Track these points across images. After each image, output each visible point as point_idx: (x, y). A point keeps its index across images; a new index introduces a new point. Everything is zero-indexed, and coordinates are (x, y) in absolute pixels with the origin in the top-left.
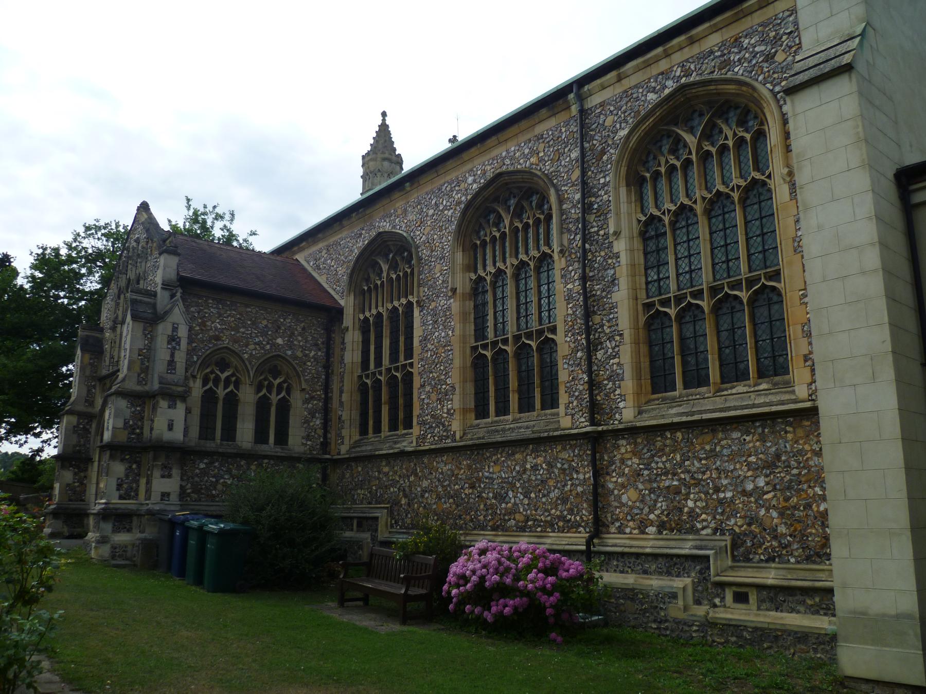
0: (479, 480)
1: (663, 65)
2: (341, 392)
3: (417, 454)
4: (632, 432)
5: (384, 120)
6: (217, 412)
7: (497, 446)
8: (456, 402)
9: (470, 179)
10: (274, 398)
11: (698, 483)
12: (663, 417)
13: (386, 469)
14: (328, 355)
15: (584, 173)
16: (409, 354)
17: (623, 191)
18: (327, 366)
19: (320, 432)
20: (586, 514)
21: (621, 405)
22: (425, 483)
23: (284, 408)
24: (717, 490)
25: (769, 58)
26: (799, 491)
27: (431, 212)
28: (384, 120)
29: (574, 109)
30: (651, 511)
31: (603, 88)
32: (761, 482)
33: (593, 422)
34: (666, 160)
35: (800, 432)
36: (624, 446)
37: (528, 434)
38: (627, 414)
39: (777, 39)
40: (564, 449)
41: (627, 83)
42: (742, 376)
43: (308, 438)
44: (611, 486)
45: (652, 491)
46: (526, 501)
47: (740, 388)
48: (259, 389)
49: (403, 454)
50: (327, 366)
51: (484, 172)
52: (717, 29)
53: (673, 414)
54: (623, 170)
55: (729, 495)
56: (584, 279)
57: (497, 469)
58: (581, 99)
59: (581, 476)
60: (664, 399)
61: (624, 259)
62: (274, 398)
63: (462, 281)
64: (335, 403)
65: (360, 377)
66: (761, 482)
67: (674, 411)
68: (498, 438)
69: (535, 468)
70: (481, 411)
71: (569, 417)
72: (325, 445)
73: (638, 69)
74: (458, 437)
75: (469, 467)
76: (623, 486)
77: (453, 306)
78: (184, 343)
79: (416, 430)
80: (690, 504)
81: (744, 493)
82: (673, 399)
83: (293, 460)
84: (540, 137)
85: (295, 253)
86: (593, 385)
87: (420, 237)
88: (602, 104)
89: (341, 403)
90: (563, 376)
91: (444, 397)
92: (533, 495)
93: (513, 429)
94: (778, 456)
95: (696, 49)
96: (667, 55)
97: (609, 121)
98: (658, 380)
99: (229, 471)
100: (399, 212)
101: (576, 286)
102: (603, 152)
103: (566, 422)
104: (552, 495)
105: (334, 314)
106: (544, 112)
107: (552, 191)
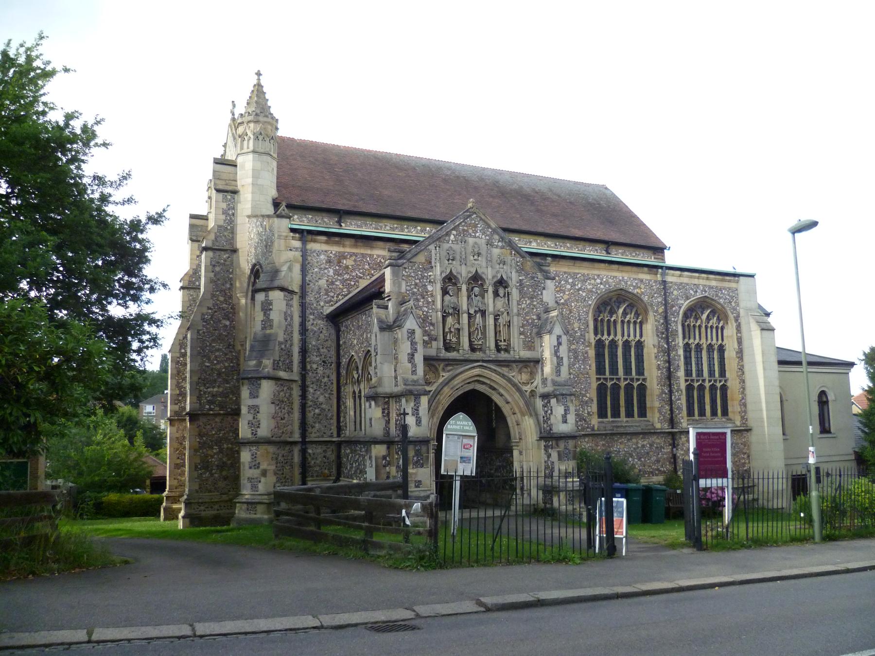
1: (696, 281)
5: (259, 79)
7: (622, 434)
9: (598, 281)
25: (730, 302)
28: (259, 79)
31: (673, 275)
37: (639, 430)
52: (715, 280)
57: (622, 446)
58: (663, 275)
68: (621, 430)
69: (643, 446)
70: (602, 414)
74: (596, 428)
77: (590, 352)
84: (642, 281)
95: (707, 283)
106: (646, 269)
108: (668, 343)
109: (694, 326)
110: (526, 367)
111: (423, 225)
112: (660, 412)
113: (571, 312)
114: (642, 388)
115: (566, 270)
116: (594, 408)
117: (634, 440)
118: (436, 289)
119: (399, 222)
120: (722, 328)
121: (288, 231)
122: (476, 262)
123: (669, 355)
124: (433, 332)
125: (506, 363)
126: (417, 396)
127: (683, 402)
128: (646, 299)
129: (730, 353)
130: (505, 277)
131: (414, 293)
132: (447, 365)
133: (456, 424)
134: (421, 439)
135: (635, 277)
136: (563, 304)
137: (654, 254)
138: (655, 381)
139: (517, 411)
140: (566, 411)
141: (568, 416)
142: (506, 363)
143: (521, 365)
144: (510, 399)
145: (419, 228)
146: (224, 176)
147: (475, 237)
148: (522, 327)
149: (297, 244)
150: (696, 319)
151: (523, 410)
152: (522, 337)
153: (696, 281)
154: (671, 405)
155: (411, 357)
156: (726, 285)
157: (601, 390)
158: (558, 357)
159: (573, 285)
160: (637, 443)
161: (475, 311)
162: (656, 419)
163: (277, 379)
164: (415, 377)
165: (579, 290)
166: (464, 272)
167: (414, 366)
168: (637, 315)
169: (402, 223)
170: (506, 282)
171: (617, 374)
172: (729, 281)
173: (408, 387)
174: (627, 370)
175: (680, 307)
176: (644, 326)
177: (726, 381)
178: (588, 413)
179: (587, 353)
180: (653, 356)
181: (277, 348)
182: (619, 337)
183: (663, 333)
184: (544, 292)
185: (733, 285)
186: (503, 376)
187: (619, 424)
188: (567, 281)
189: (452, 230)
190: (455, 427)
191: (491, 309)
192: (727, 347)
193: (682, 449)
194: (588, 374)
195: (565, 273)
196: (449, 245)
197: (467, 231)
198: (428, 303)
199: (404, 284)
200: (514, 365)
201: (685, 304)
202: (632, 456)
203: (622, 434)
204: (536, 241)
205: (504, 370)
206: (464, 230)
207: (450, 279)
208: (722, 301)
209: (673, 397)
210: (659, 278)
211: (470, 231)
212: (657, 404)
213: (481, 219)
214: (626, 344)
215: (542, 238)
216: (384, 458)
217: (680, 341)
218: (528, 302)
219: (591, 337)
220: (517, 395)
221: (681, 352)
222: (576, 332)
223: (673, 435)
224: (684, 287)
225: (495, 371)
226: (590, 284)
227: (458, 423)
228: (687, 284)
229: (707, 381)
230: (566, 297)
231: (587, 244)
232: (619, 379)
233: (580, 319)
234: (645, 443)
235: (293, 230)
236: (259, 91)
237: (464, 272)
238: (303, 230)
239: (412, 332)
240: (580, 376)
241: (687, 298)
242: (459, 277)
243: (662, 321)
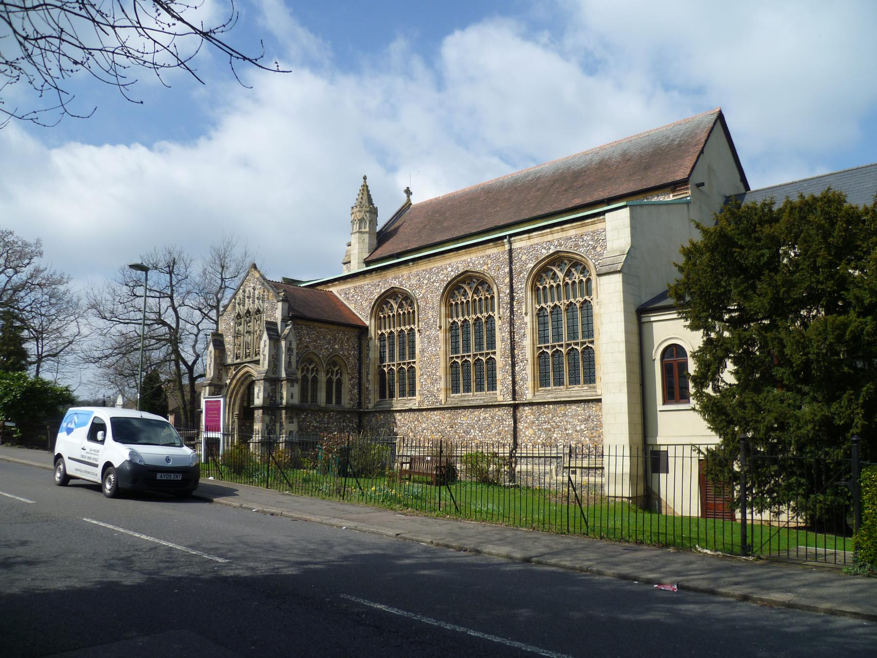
0: (455, 424)
2: (368, 374)
3: (420, 410)
4: (531, 404)
6: (307, 386)
8: (442, 384)
9: (450, 269)
10: (335, 378)
11: (558, 427)
14: (360, 353)
16: (412, 355)
17: (529, 293)
18: (360, 360)
19: (357, 396)
20: (510, 440)
22: (424, 425)
23: (339, 383)
24: (566, 430)
25: (594, 248)
27: (426, 282)
29: (507, 247)
31: (521, 240)
32: (583, 427)
33: (514, 399)
34: (549, 282)
37: (481, 403)
38: (529, 396)
39: (597, 241)
43: (351, 400)
45: (539, 430)
47: (576, 388)
48: (327, 374)
49: (411, 410)
50: (360, 360)
51: (457, 268)
53: (549, 398)
54: (530, 283)
57: (465, 419)
61: (529, 326)
62: (335, 378)
63: (445, 322)
64: (364, 380)
65: (380, 366)
66: (583, 427)
68: (465, 404)
69: (485, 419)
71: (502, 394)
72: (360, 404)
73: (538, 236)
75: (450, 418)
78: (295, 351)
79: (418, 398)
82: (549, 391)
83: (344, 412)
85: (329, 287)
86: (514, 383)
87: (418, 294)
88: (520, 248)
89: (368, 381)
90: (499, 376)
91: (434, 382)
94: (589, 417)
97: (524, 258)
98: (542, 380)
99: (315, 419)
100: (405, 277)
101: (507, 335)
102: (521, 272)
103: (500, 398)
105: (364, 330)
107: (495, 287)
112: (502, 384)
114: (491, 362)
115: (424, 268)
135: (482, 254)
156: (590, 228)
157: (453, 367)
159: (429, 279)
172: (593, 223)
179: (438, 336)
185: (600, 226)
202: (473, 427)
230: (424, 291)
236: (365, 189)
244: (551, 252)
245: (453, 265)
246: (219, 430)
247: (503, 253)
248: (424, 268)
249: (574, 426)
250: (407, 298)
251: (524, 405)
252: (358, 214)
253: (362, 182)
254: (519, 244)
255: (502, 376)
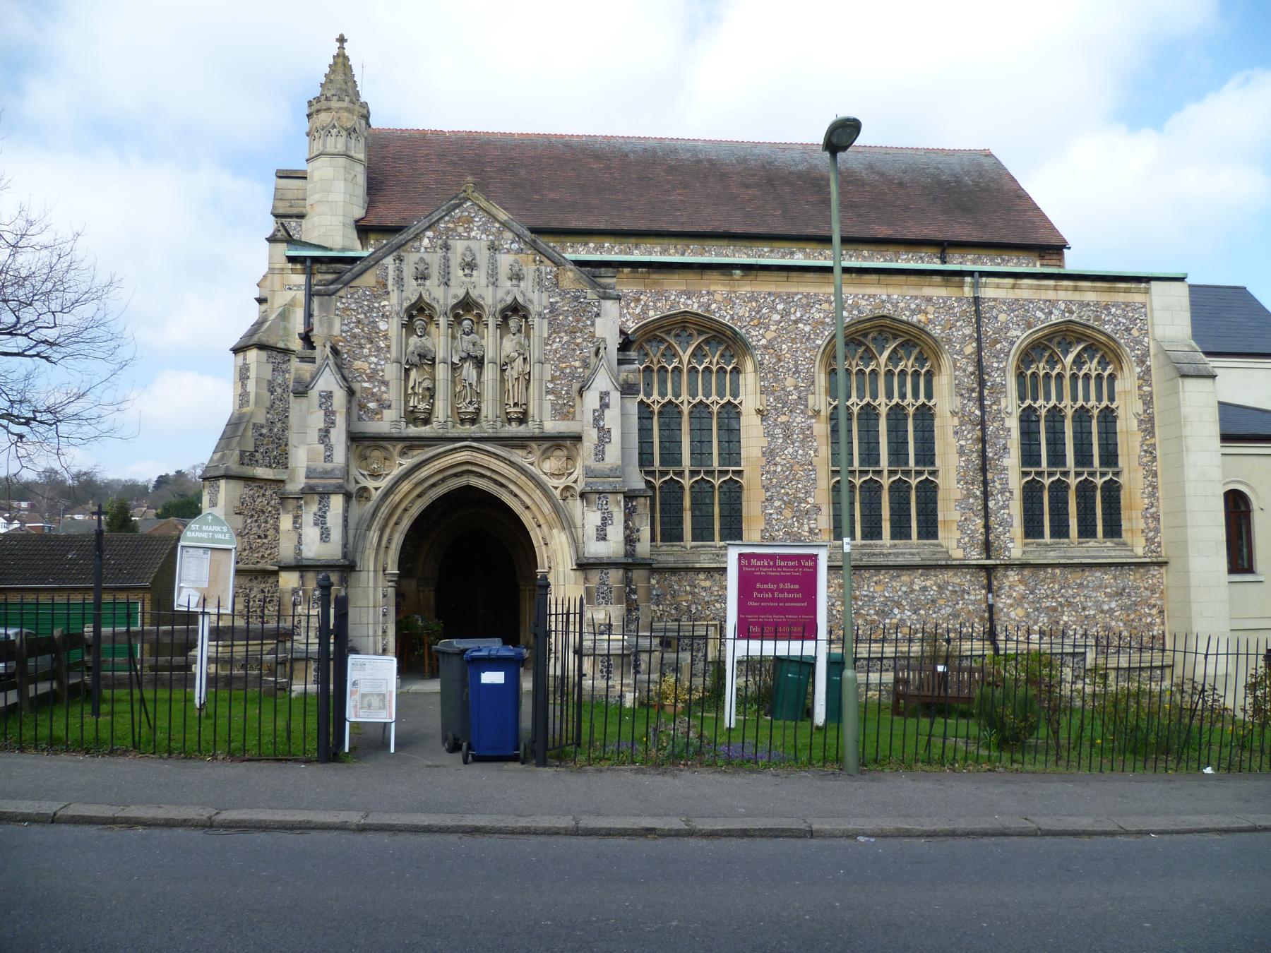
1: (1051, 295)
7: (878, 568)
11: (1070, 604)
12: (1046, 558)
13: (708, 584)
15: (979, 350)
21: (1011, 545)
24: (1084, 609)
25: (1128, 330)
26: (1136, 611)
27: (776, 317)
30: (1036, 623)
31: (998, 286)
35: (1138, 576)
36: (1013, 576)
37: (916, 560)
40: (955, 575)
41: (1018, 294)
42: (1093, 534)
44: (1001, 605)
45: (1037, 609)
46: (914, 617)
47: (1092, 543)
52: (1094, 290)
53: (1052, 557)
55: (1092, 612)
56: (983, 441)
57: (878, 588)
59: (972, 598)
60: (1039, 545)
66: (1113, 605)
67: (1051, 554)
68: (880, 561)
69: (924, 589)
73: (1031, 287)
76: (1011, 605)
80: (1065, 618)
81: (1102, 611)
84: (929, 300)
87: (757, 337)
88: (995, 300)
92: (922, 612)
93: (896, 555)
94: (1124, 589)
95: (1077, 296)
96: (1055, 288)
97: (1002, 317)
98: (1032, 529)
100: (718, 297)
102: (996, 341)
103: (957, 554)
104: (943, 612)
106: (937, 279)
108: (982, 407)
109: (1047, 376)
110: (559, 447)
111: (597, 239)
112: (961, 528)
113: (780, 360)
114: (929, 492)
115: (772, 289)
116: (824, 521)
117: (905, 578)
118: (391, 327)
119: (557, 239)
120: (1112, 377)
121: (284, 259)
122: (468, 279)
123: (983, 430)
124: (385, 396)
125: (519, 442)
126: (324, 495)
127: (1016, 509)
128: (936, 331)
129: (1127, 425)
130: (520, 300)
131: (354, 336)
132: (411, 448)
133: (201, 530)
134: (324, 563)
135: (915, 293)
136: (765, 347)
137: (1042, 257)
138: (953, 476)
139: (542, 521)
140: (605, 521)
141: (609, 529)
142: (519, 442)
143: (546, 445)
144: (529, 502)
145: (592, 245)
146: (289, 195)
147: (469, 238)
148: (552, 381)
149: (300, 279)
150: (1052, 362)
151: (550, 518)
152: (551, 397)
153: (1051, 295)
154: (986, 517)
155: (325, 435)
156: (1121, 298)
158: (600, 429)
160: (912, 583)
161: (461, 359)
162: (954, 540)
163: (249, 480)
164: (329, 466)
165: (796, 322)
166: (442, 296)
167: (329, 448)
168: (921, 360)
169: (563, 239)
170: (524, 308)
171: (877, 463)
172: (1127, 291)
173: (313, 482)
174: (898, 454)
175: (1012, 343)
176: (935, 380)
177: (1117, 474)
178: (811, 531)
179: (810, 428)
180: (950, 431)
181: (250, 433)
182: (882, 399)
183: (973, 390)
184: (598, 320)
185: (1137, 298)
186: (512, 464)
187: (877, 551)
188: (773, 309)
189: (426, 229)
190: (199, 535)
191: (489, 355)
192: (1120, 413)
193: (1009, 597)
194: (811, 463)
195: (770, 294)
196: (419, 255)
197: (454, 230)
198: (379, 349)
199: (337, 321)
200: (534, 445)
201: (1021, 337)
202: (898, 605)
203: (878, 568)
204: (802, 250)
205: (518, 456)
206: (448, 229)
207: (418, 313)
208: (1108, 328)
209: (991, 504)
210: (968, 292)
211: (460, 229)
212: (957, 516)
213: (481, 208)
214: (897, 414)
215: (814, 245)
216: (295, 592)
217: (1011, 404)
218: (565, 339)
219: (820, 400)
220: (538, 495)
221: (1013, 423)
222: (790, 393)
223: (989, 570)
224: (1022, 306)
225: (497, 456)
226: (819, 311)
227: (204, 528)
228: (1031, 301)
229: (1072, 474)
230: (770, 335)
231: (902, 249)
232: (879, 473)
233: (797, 372)
234: (928, 583)
235: (292, 259)
236: (341, 63)
237: (442, 296)
238: (306, 258)
239: (328, 396)
240: (796, 467)
241: (1029, 326)
242: (436, 306)
243: (971, 369)
244: (1054, 319)
245: (866, 299)
246: (809, 632)
247: (959, 300)
248: (772, 289)
249: (1098, 605)
250: (725, 340)
251: (1008, 566)
252: (345, 115)
253: (334, 48)
254: (992, 291)
255: (949, 511)
